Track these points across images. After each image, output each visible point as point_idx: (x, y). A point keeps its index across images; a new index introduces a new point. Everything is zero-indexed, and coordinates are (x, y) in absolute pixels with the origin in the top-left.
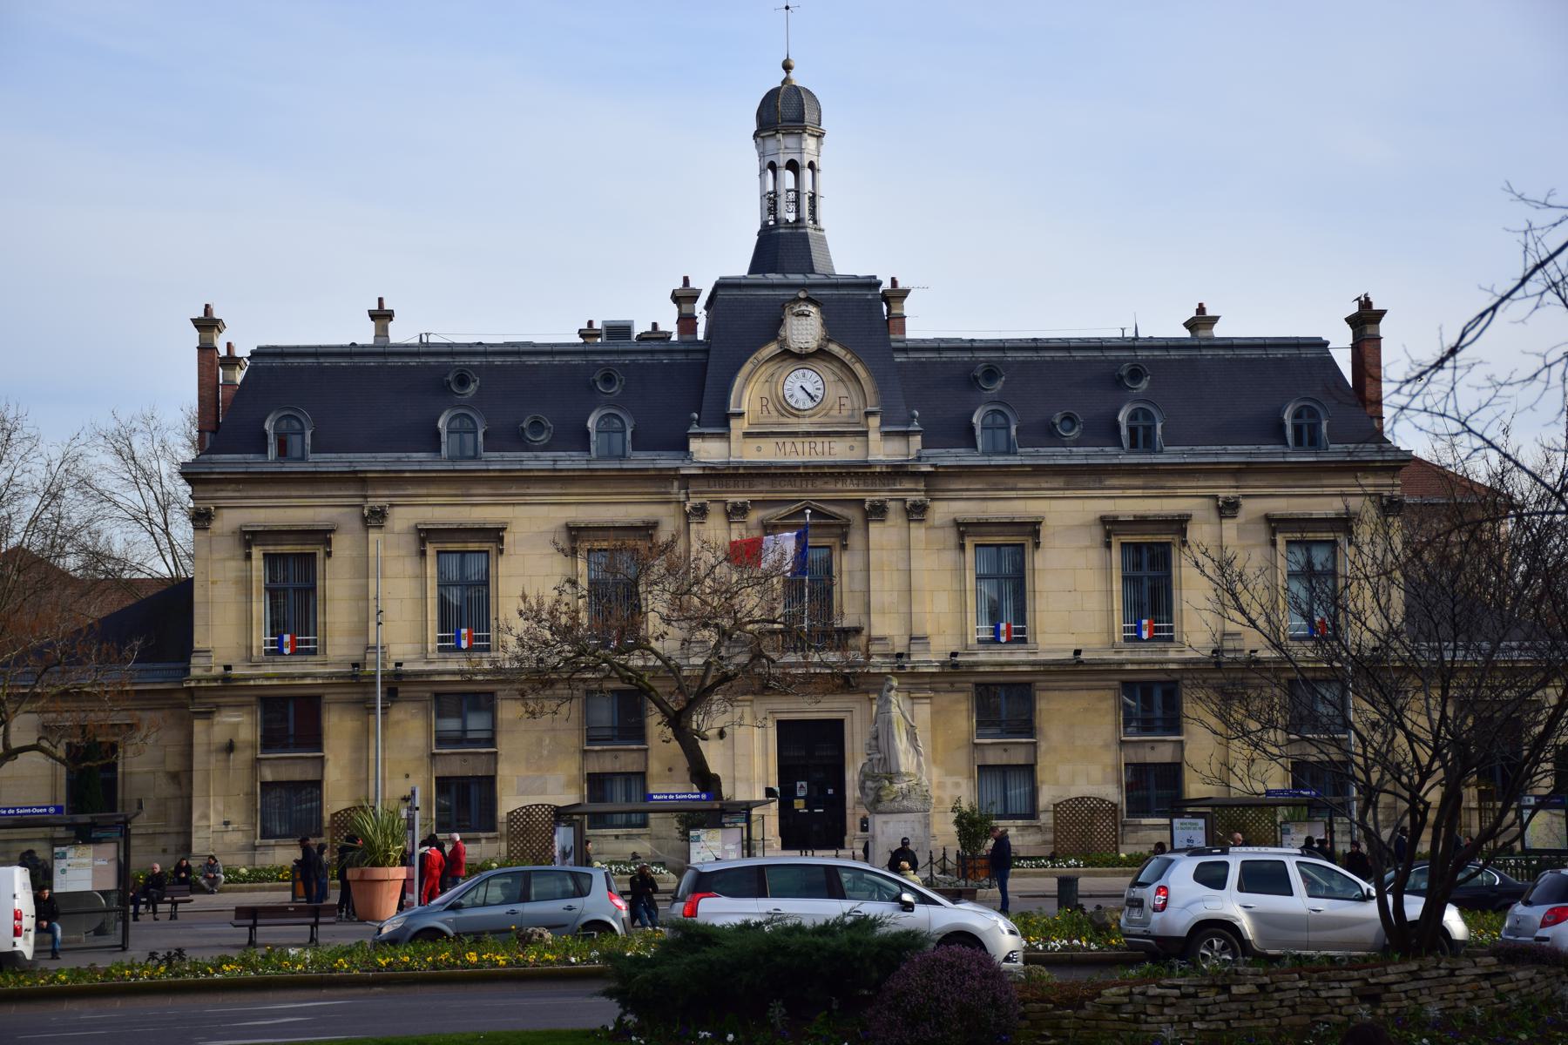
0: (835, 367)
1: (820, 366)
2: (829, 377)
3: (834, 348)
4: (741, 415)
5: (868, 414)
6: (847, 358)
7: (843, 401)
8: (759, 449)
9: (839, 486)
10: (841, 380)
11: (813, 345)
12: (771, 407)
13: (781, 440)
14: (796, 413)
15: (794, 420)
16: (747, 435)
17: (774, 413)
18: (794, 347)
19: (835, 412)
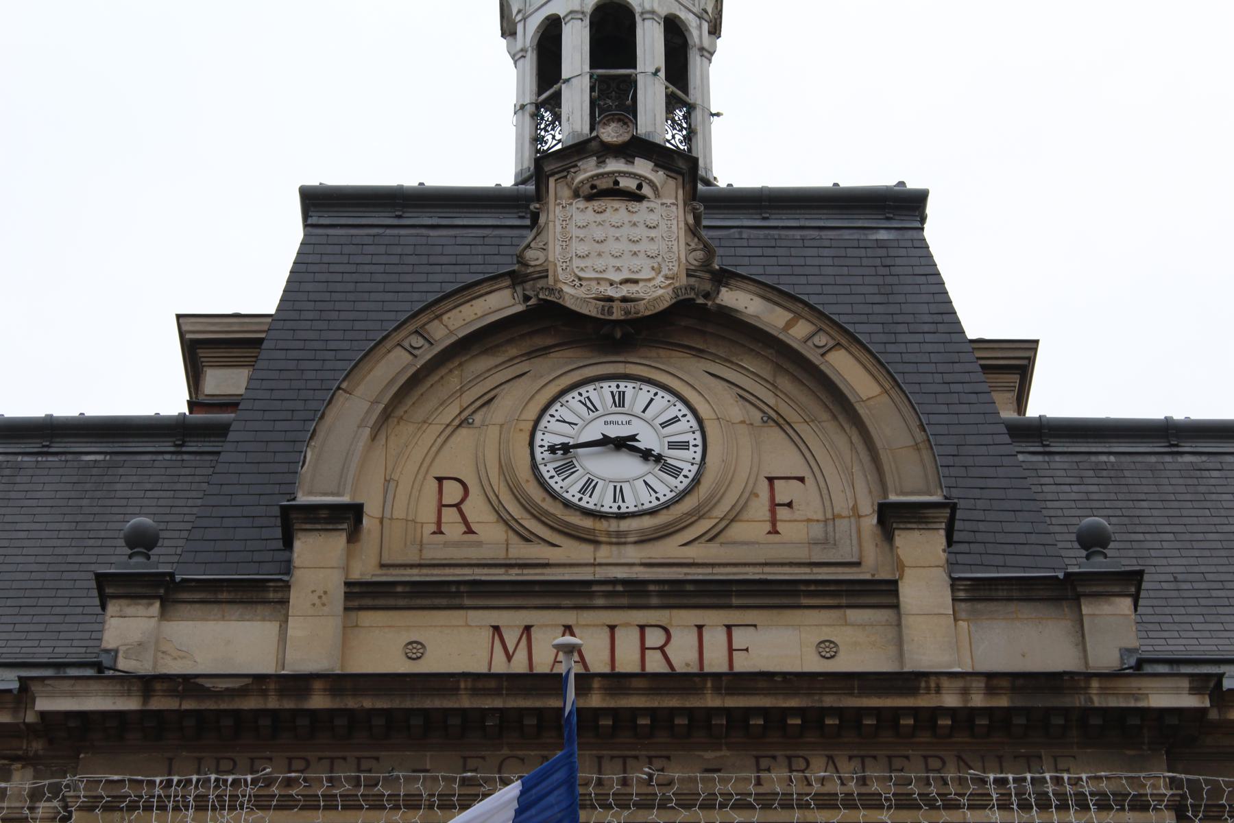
0: (752, 373)
1: (690, 371)
2: (720, 403)
3: (741, 300)
4: (348, 517)
5: (892, 517)
6: (799, 333)
7: (784, 492)
8: (415, 650)
9: (777, 780)
10: (777, 421)
11: (655, 291)
12: (476, 508)
13: (512, 621)
14: (589, 525)
15: (584, 552)
16: (364, 595)
17: (492, 534)
18: (574, 296)
19: (752, 529)
